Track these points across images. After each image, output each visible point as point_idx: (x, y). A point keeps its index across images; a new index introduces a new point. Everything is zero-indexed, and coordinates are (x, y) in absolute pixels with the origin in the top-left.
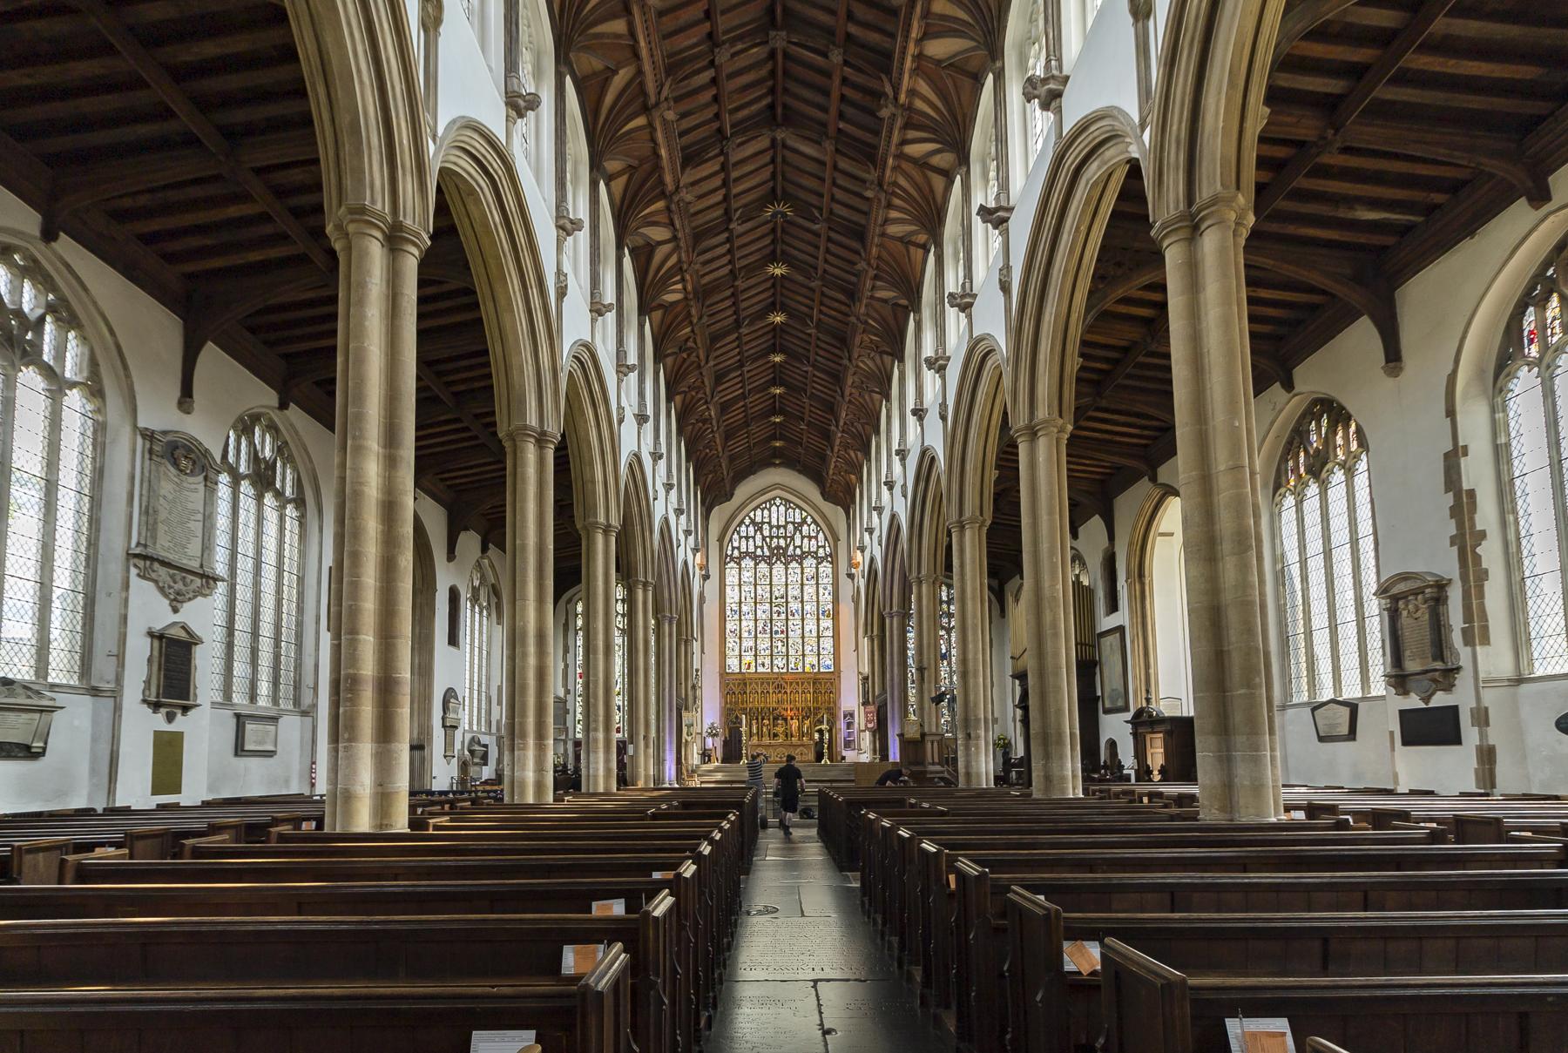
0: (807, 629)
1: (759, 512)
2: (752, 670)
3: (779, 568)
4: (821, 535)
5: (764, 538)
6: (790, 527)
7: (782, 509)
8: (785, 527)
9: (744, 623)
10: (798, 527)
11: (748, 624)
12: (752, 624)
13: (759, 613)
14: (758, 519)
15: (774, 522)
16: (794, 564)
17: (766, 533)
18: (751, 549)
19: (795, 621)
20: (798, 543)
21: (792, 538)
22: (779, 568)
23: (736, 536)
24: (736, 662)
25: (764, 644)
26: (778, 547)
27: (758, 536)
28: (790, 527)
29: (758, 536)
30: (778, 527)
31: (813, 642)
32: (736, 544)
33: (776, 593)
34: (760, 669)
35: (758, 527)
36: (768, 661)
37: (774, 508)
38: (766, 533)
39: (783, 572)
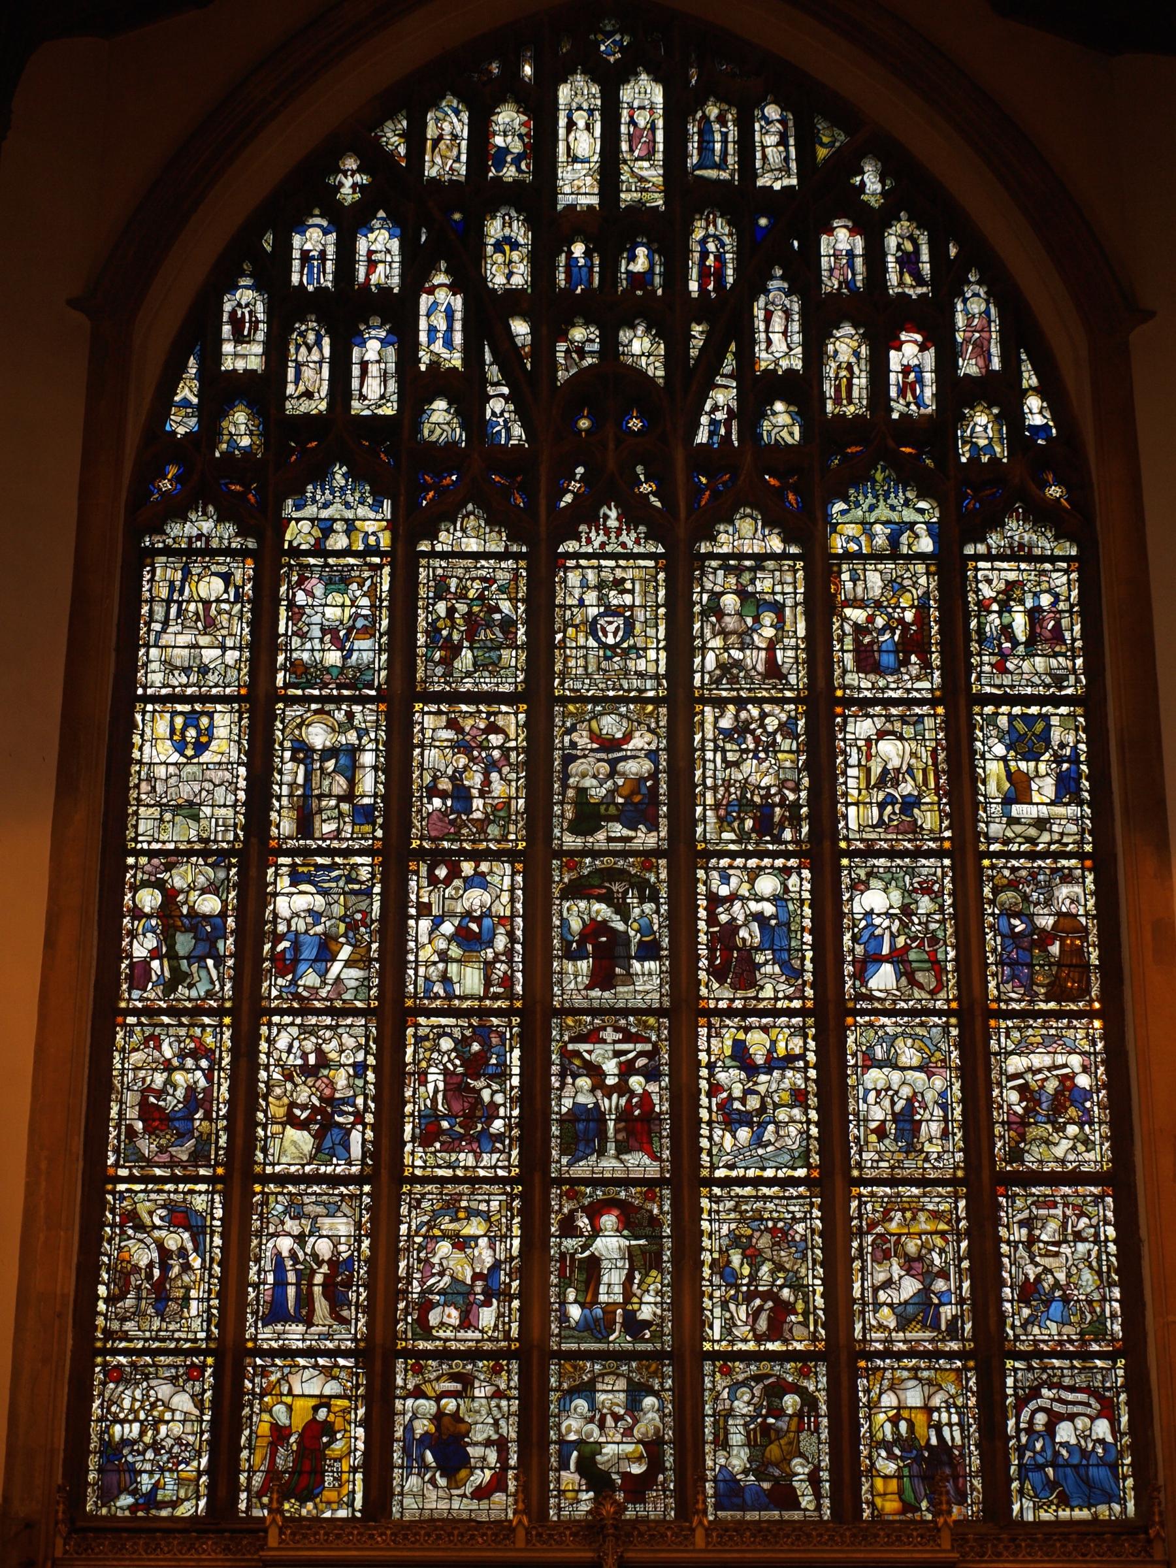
0: (875, 1094)
1: (450, 123)
2: (343, 1498)
3: (608, 576)
4: (973, 308)
5: (485, 314)
6: (713, 237)
7: (644, 96)
8: (667, 231)
9: (283, 1041)
10: (778, 236)
11: (315, 1050)
12: (348, 1045)
13: (426, 940)
14: (446, 162)
15: (577, 186)
16: (746, 535)
17: (508, 272)
18: (375, 393)
19: (755, 1048)
20: (779, 346)
21: (733, 323)
22: (608, 576)
23: (246, 298)
24: (181, 1407)
25: (467, 1248)
26: (613, 378)
27: (440, 308)
28: (713, 237)
29: (440, 308)
30: (612, 226)
31: (930, 1223)
32: (244, 357)
33: (589, 776)
34: (420, 1495)
35: (443, 229)
36: (488, 1415)
37: (575, 95)
38: (508, 272)
39: (642, 591)
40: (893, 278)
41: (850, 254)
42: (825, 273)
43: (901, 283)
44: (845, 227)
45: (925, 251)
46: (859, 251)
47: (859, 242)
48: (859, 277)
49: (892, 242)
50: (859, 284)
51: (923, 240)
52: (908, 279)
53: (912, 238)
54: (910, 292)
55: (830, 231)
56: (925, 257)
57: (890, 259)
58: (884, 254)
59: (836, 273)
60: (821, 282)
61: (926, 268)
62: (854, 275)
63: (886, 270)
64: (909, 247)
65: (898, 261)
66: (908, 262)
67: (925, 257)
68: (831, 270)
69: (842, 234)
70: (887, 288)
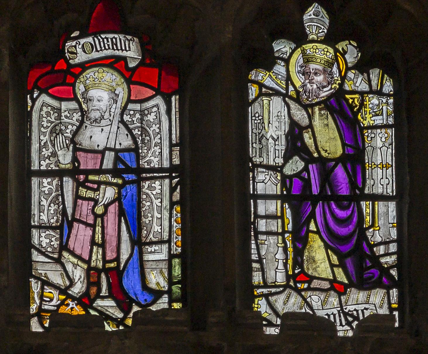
40: (271, 256)
41: (129, 170)
42: (42, 239)
43: (299, 278)
44: (116, 63)
45: (381, 149)
46: (159, 154)
47: (161, 124)
48: (156, 255)
49: (271, 121)
50: (156, 279)
51: (377, 112)
52: (320, 259)
53: (341, 109)
54: (324, 306)
55: (63, 79)
56: (381, 178)
57: (265, 183)
58: (244, 166)
59: (80, 236)
60: (26, 268)
61: (383, 223)
62: (138, 243)
63: (246, 228)
64: (327, 138)
65: (297, 196)
66: (324, 193)
67: (381, 178)
68: (65, 225)
69: (102, 90)
70: (249, 294)
